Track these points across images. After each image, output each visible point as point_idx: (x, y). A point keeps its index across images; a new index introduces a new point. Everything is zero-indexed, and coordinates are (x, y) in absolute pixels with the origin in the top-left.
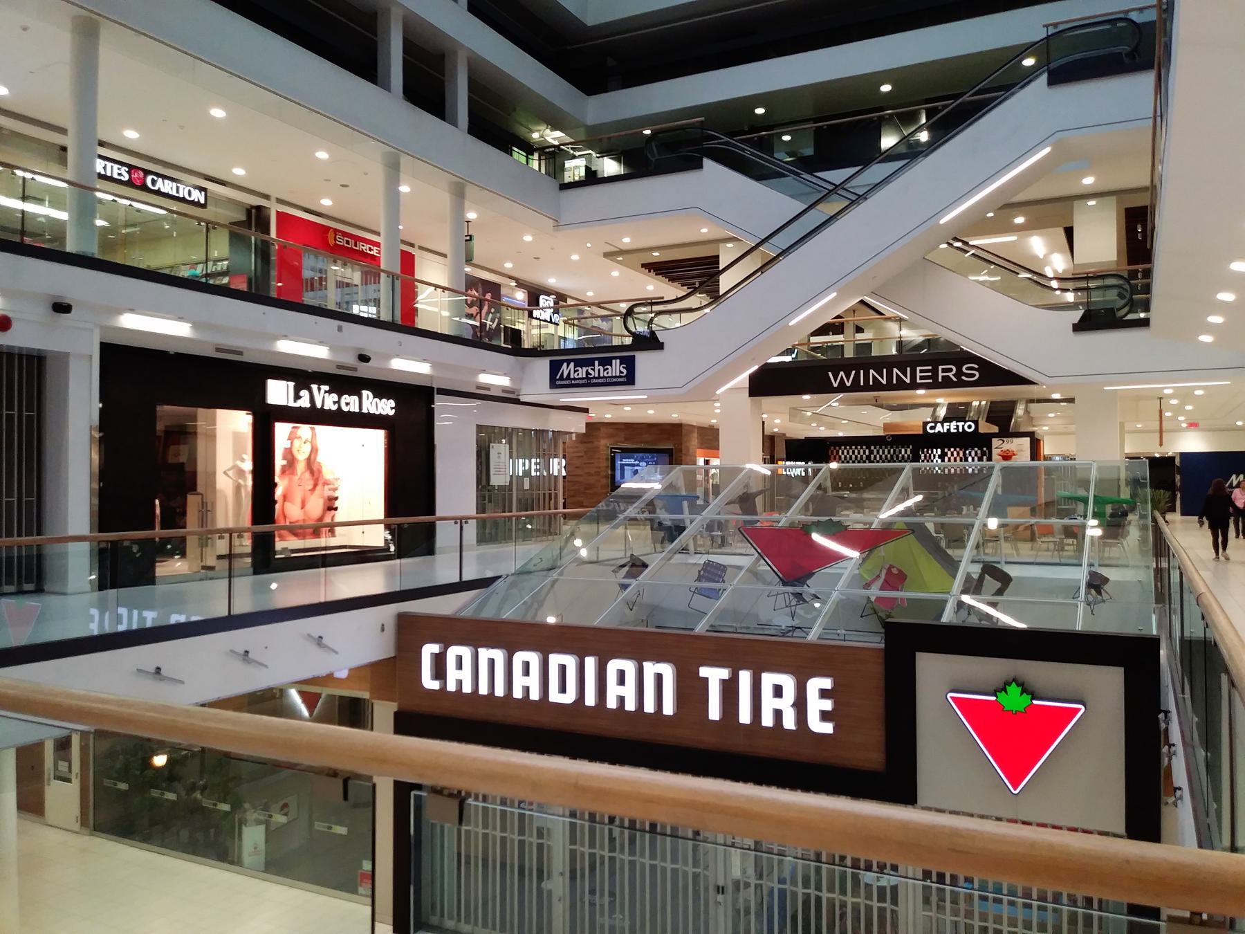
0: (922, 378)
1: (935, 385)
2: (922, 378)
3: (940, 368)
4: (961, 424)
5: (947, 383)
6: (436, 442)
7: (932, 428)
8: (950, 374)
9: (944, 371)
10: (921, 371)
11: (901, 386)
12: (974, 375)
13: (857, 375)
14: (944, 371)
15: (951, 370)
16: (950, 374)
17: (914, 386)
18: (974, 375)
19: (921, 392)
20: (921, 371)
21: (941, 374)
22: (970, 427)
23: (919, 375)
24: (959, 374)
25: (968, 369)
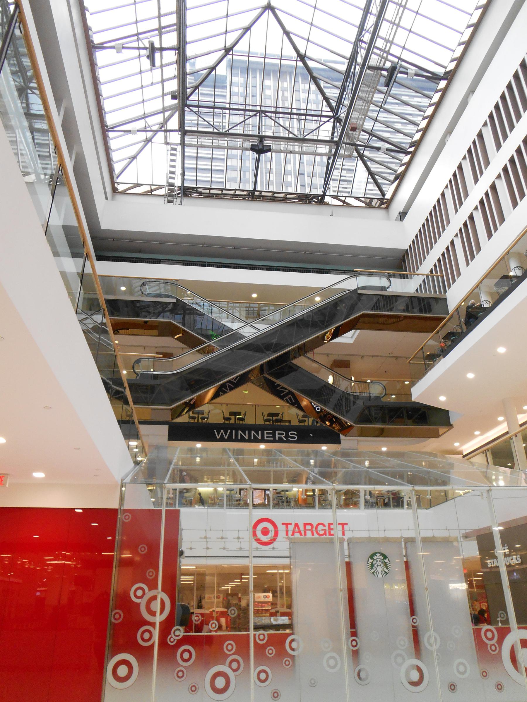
0: (267, 437)
1: (274, 441)
2: (267, 437)
3: (277, 432)
5: (281, 441)
8: (282, 436)
9: (279, 434)
10: (267, 433)
11: (256, 440)
12: (295, 438)
13: (231, 433)
14: (279, 434)
15: (283, 434)
16: (282, 436)
17: (263, 441)
18: (295, 438)
20: (267, 433)
21: (277, 436)
23: (265, 435)
24: (287, 436)
25: (291, 434)
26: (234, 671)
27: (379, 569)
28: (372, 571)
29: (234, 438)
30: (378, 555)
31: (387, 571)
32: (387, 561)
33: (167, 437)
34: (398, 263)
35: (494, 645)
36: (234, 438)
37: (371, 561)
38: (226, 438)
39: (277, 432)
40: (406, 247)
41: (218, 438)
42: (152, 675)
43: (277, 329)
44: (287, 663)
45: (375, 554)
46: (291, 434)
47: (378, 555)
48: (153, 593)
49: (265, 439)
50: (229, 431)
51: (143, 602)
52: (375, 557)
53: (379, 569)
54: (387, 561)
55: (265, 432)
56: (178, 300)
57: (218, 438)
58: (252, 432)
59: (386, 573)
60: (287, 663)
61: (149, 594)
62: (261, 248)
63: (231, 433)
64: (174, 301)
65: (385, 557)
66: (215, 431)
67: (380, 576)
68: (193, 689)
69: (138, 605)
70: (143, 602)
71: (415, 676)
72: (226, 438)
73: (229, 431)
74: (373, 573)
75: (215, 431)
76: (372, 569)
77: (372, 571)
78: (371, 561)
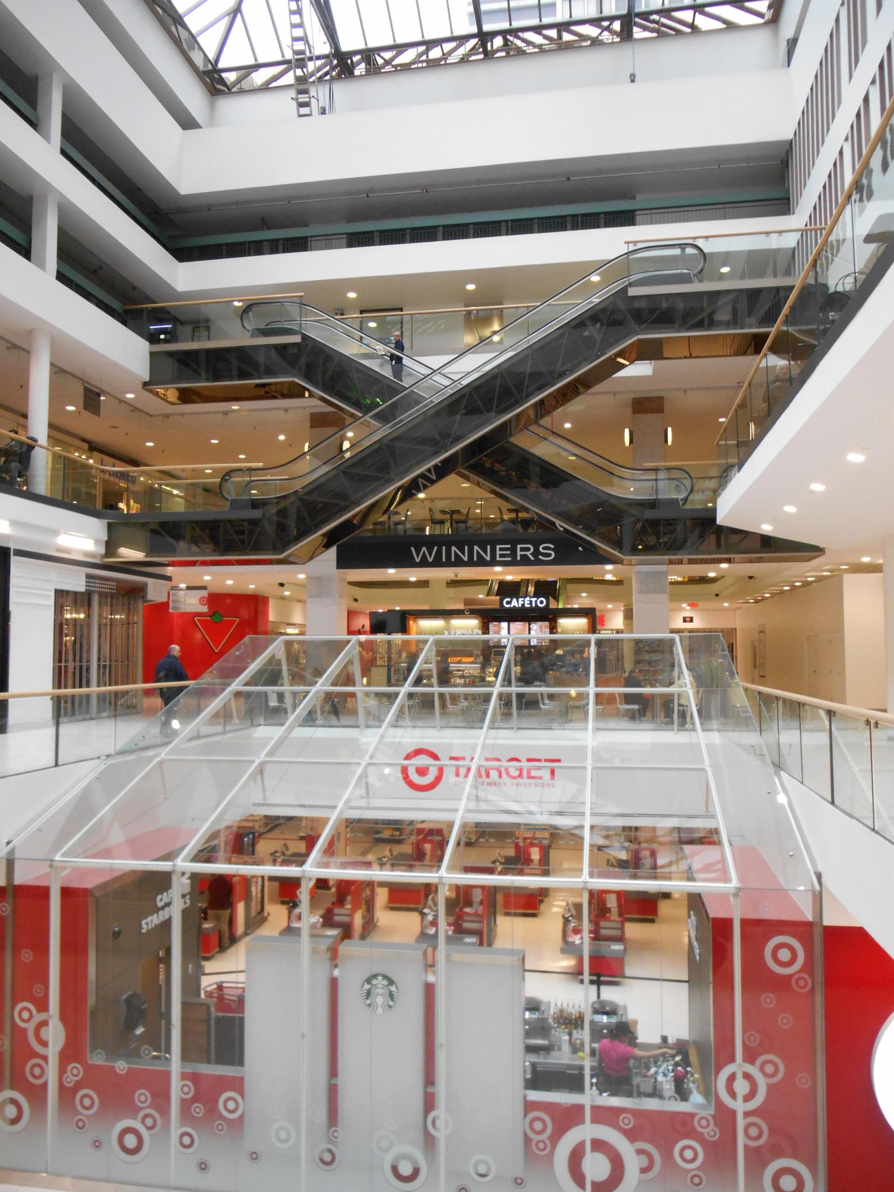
0: (501, 556)
1: (514, 563)
2: (501, 556)
3: (519, 546)
4: (534, 600)
5: (525, 561)
6: (12, 607)
7: (508, 603)
8: (528, 553)
9: (522, 549)
10: (501, 549)
11: (481, 562)
12: (550, 555)
14: (522, 549)
15: (528, 549)
16: (528, 553)
17: (493, 562)
18: (550, 555)
19: (498, 569)
20: (501, 549)
21: (519, 553)
22: (542, 602)
23: (498, 552)
24: (536, 553)
25: (543, 548)
26: (149, 1128)
27: (380, 1000)
28: (368, 1002)
29: (444, 560)
30: (380, 978)
31: (391, 1003)
32: (393, 988)
33: (334, 563)
34: (762, 179)
35: (543, 1141)
36: (444, 560)
37: (367, 987)
38: (430, 560)
39: (519, 546)
40: (790, 136)
41: (418, 560)
42: (45, 1122)
43: (463, 392)
44: (220, 1127)
45: (375, 976)
46: (543, 548)
47: (380, 978)
48: (42, 1016)
49: (498, 559)
50: (436, 548)
51: (30, 1027)
52: (374, 982)
53: (380, 1000)
54: (393, 988)
55: (498, 547)
56: (305, 337)
57: (418, 560)
58: (476, 548)
59: (390, 1007)
60: (220, 1127)
61: (38, 1017)
62: (479, 182)
63: (439, 552)
64: (297, 339)
65: (391, 982)
66: (412, 549)
67: (380, 1010)
68: (97, 1144)
69: (25, 1030)
70: (30, 1027)
71: (406, 1169)
72: (430, 560)
73: (436, 548)
74: (369, 1005)
75: (412, 549)
76: (367, 998)
77: (368, 1002)
78: (367, 987)
